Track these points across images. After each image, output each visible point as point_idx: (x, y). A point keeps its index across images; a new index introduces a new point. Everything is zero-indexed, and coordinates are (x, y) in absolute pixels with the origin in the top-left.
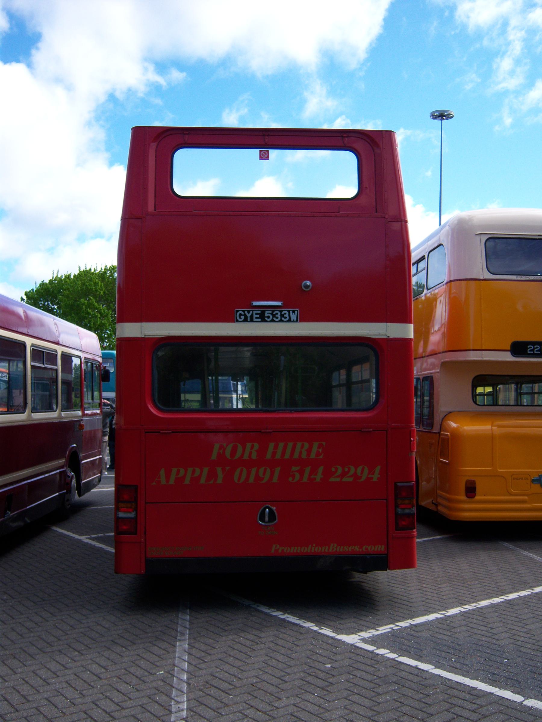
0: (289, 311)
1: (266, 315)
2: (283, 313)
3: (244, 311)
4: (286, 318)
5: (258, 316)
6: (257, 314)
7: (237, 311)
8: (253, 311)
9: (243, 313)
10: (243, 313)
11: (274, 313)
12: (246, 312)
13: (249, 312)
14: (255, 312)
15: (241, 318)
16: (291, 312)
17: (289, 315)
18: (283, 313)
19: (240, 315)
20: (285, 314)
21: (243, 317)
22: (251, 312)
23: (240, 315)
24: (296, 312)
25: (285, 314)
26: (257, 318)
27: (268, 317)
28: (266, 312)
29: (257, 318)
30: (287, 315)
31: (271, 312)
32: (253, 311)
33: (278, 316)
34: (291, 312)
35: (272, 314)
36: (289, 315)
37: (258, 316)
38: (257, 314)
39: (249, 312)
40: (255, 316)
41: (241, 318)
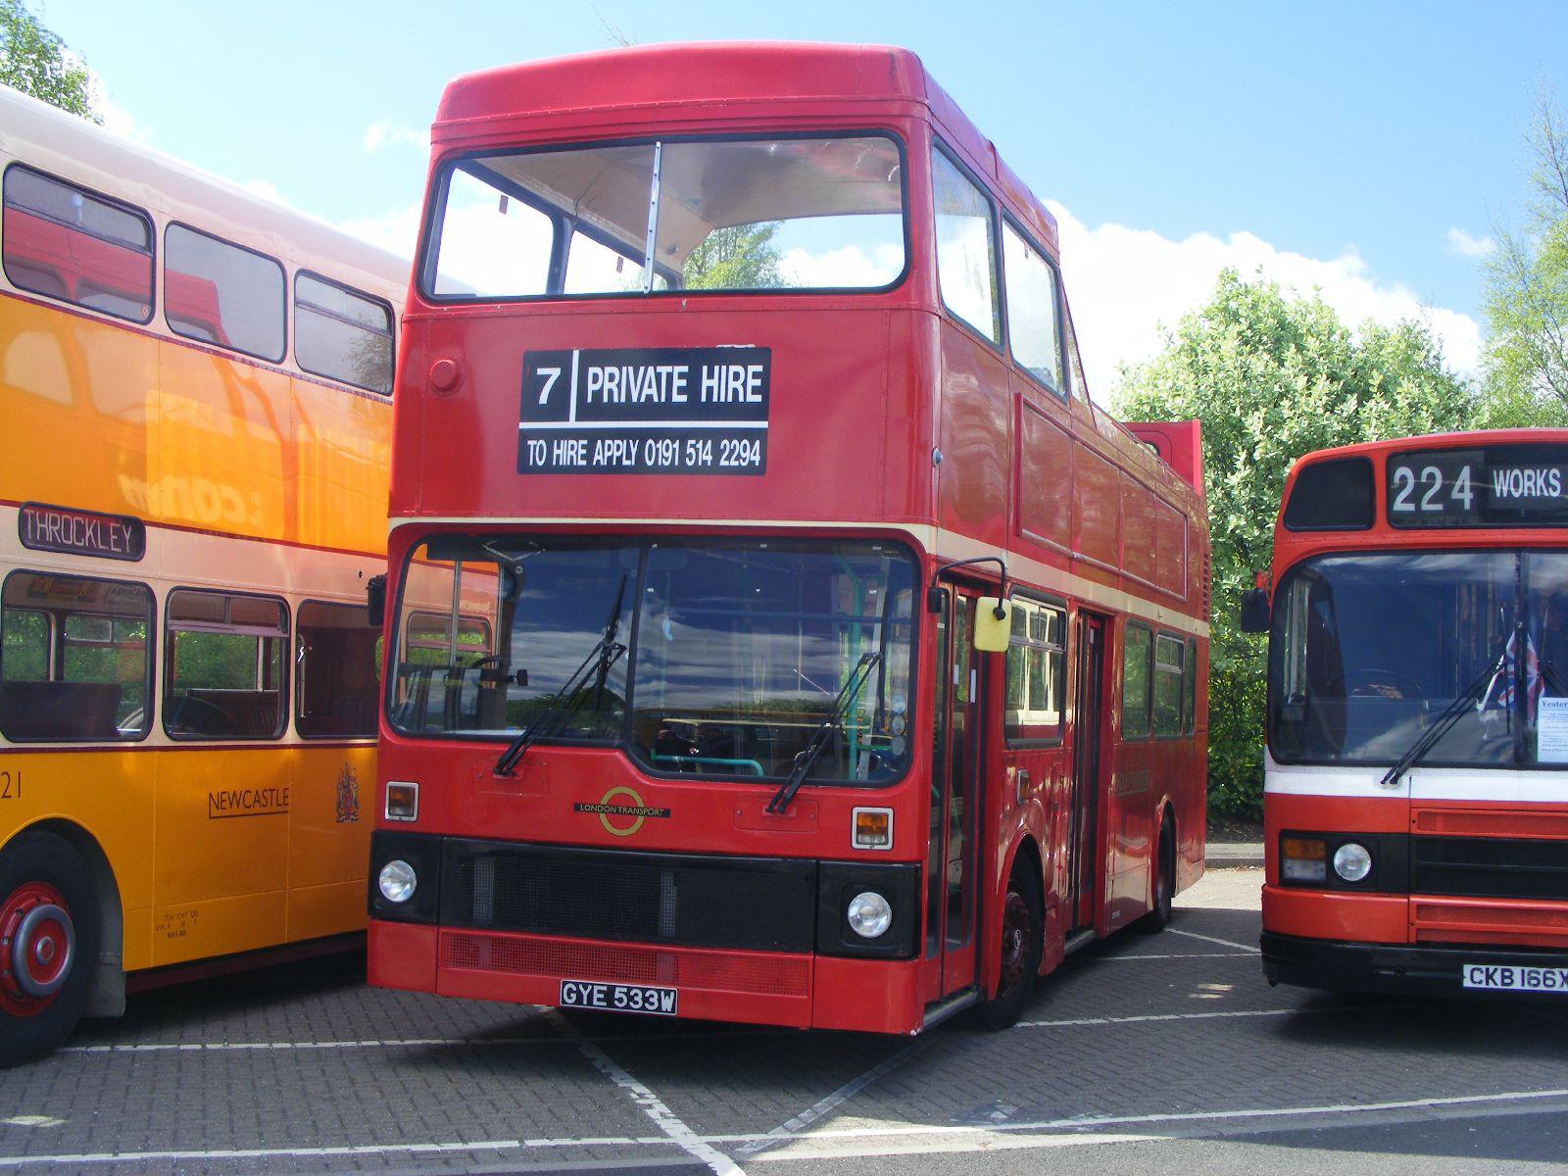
0: (659, 992)
1: (617, 995)
2: (647, 995)
3: (577, 984)
4: (652, 1004)
5: (602, 996)
6: (599, 992)
7: (565, 983)
9: (575, 989)
10: (575, 989)
11: (632, 994)
12: (581, 986)
14: (596, 988)
15: (570, 997)
16: (663, 993)
17: (659, 1000)
18: (647, 995)
19: (570, 990)
20: (652, 996)
21: (574, 996)
22: (590, 987)
23: (570, 990)
24: (672, 994)
25: (652, 996)
26: (599, 1000)
27: (621, 1000)
28: (618, 990)
30: (654, 1000)
31: (625, 990)
32: (593, 985)
33: (638, 999)
34: (663, 993)
35: (627, 994)
36: (659, 1000)
37: (602, 996)
38: (599, 992)
39: (585, 986)
40: (596, 995)
41: (570, 997)
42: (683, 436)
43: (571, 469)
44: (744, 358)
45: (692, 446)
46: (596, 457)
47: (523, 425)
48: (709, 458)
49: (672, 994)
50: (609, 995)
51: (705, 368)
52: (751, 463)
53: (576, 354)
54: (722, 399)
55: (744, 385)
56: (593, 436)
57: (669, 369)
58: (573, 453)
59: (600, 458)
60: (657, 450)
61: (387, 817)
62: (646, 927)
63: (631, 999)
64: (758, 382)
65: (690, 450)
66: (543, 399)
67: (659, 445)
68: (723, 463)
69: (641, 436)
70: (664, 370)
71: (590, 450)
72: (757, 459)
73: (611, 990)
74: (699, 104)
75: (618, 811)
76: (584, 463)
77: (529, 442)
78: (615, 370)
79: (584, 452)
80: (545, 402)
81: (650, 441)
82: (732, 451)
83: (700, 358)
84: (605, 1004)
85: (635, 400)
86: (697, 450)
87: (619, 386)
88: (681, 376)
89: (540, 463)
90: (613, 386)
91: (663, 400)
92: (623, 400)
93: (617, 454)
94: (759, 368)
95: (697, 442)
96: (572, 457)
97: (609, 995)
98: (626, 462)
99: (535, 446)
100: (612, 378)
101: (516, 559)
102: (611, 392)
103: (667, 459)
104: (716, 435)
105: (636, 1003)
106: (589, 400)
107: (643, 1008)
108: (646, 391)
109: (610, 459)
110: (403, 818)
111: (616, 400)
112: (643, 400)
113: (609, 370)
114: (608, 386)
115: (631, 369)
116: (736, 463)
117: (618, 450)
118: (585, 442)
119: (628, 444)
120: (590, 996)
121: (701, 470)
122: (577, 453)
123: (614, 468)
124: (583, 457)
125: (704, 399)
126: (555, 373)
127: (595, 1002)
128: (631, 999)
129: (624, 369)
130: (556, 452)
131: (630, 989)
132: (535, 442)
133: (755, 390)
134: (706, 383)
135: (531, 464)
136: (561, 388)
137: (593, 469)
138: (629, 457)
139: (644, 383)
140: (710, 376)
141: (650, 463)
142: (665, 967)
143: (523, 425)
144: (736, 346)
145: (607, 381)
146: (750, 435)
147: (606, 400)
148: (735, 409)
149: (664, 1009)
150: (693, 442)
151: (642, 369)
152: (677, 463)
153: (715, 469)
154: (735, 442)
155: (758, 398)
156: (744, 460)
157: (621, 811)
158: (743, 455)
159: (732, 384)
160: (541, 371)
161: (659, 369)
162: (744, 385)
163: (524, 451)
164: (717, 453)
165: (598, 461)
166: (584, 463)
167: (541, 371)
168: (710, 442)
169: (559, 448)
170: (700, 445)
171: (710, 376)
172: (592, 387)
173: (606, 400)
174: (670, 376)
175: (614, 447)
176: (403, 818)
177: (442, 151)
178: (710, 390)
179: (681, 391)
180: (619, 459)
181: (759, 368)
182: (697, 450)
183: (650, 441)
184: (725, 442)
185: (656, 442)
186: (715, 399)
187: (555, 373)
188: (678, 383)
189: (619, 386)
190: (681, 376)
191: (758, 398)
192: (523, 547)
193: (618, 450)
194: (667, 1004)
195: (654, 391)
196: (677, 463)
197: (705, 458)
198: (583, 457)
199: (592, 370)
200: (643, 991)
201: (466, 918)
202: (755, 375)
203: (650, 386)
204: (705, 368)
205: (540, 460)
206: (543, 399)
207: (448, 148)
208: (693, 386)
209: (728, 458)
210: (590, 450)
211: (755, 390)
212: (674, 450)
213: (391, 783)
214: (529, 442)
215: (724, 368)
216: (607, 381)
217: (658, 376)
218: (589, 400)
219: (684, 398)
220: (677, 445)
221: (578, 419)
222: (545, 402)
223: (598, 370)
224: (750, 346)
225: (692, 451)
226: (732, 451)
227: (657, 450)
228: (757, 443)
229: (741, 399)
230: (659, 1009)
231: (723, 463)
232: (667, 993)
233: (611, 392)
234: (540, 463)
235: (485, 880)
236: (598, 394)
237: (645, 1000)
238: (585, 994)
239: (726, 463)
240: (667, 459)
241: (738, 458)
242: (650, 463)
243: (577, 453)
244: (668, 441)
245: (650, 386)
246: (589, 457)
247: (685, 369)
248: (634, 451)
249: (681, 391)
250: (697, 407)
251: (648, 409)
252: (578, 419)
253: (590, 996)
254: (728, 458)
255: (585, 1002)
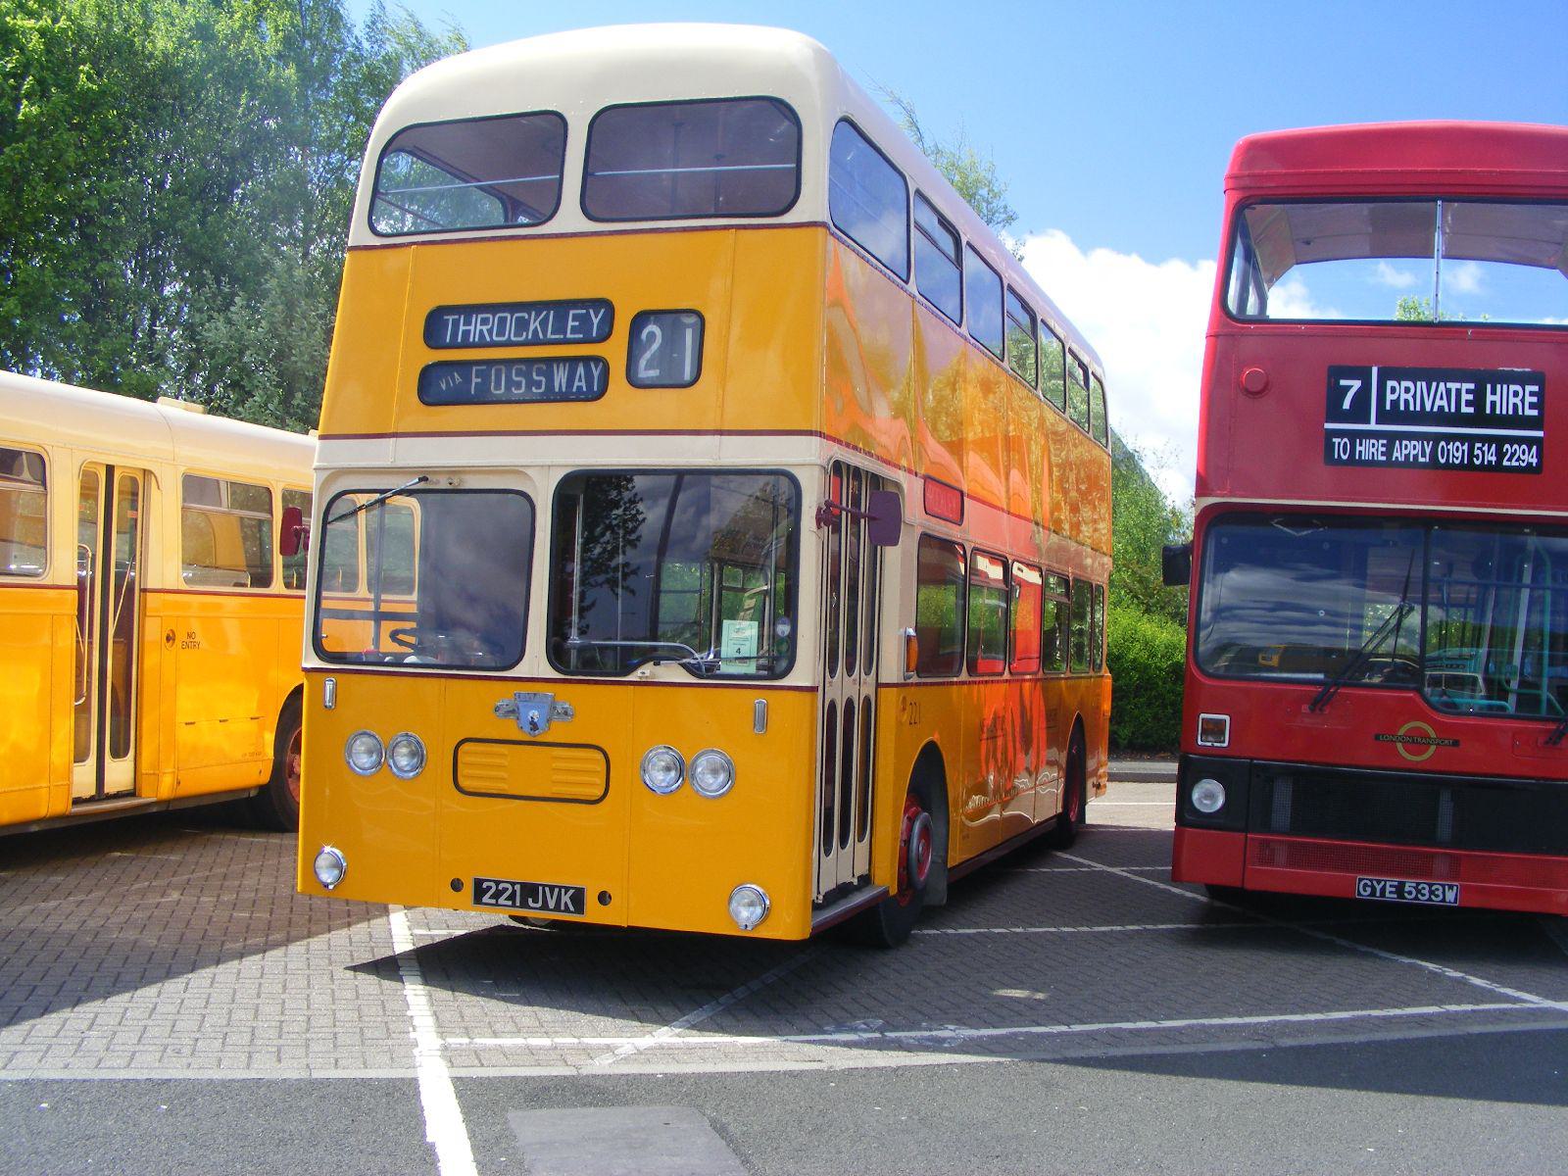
0: (1443, 886)
1: (1407, 889)
3: (1371, 880)
4: (1437, 896)
5: (1394, 889)
6: (1391, 886)
7: (1361, 880)
8: (1385, 881)
9: (1369, 883)
10: (1369, 883)
11: (1420, 887)
12: (1375, 882)
13: (1379, 882)
14: (1388, 884)
15: (1365, 890)
18: (1433, 888)
19: (1366, 885)
20: (1437, 889)
21: (1369, 890)
22: (1383, 883)
23: (1366, 885)
24: (1455, 888)
25: (1437, 889)
26: (1391, 892)
27: (1410, 893)
28: (1407, 885)
29: (1391, 892)
30: (1440, 893)
31: (1414, 885)
32: (1385, 881)
33: (1426, 892)
35: (1416, 888)
37: (1394, 889)
38: (1391, 886)
39: (1379, 882)
40: (1388, 889)
41: (1365, 890)
42: (1471, 440)
43: (1372, 463)
44: (1523, 380)
45: (1478, 448)
46: (1395, 454)
47: (1328, 426)
48: (1494, 459)
49: (1455, 888)
50: (1400, 889)
51: (1489, 386)
52: (1530, 464)
53: (1375, 370)
54: (1504, 412)
55: (1523, 401)
56: (1392, 438)
57: (1458, 385)
58: (1374, 450)
59: (1398, 455)
60: (1448, 450)
61: (1200, 743)
62: (1430, 839)
63: (1419, 891)
64: (1534, 399)
65: (1476, 452)
66: (1346, 405)
67: (1450, 447)
68: (1505, 463)
69: (1436, 438)
70: (1454, 386)
71: (1390, 448)
72: (1534, 461)
73: (1402, 885)
74: (1475, 172)
75: (1413, 740)
76: (1384, 458)
77: (1334, 440)
78: (1410, 384)
79: (1384, 449)
80: (1348, 408)
81: (1443, 443)
82: (1513, 455)
83: (1483, 380)
84: (1395, 896)
85: (1428, 409)
86: (1483, 452)
87: (1414, 397)
88: (1468, 391)
89: (1345, 457)
90: (1409, 397)
91: (1453, 410)
92: (1418, 408)
93: (1413, 452)
94: (1535, 388)
95: (1483, 446)
96: (1373, 453)
97: (1400, 889)
98: (1421, 460)
99: (1339, 444)
100: (1407, 390)
101: (1300, 534)
102: (1406, 402)
103: (1457, 458)
104: (1500, 441)
105: (1423, 895)
106: (1388, 407)
107: (1430, 899)
108: (1438, 403)
109: (1407, 456)
110: (1216, 744)
111: (1412, 408)
112: (1435, 409)
113: (1404, 384)
114: (1403, 396)
115: (1424, 384)
116: (1517, 464)
117: (1414, 449)
118: (1385, 442)
119: (1423, 443)
120: (1383, 890)
121: (1487, 468)
122: (1377, 450)
123: (1410, 464)
124: (1383, 454)
125: (1488, 411)
126: (1356, 384)
127: (1387, 895)
128: (1419, 891)
129: (1419, 383)
130: (1358, 448)
131: (1418, 884)
132: (1340, 440)
133: (1532, 406)
134: (1489, 398)
135: (1336, 456)
136: (1363, 396)
137: (1390, 463)
138: (1424, 455)
139: (1437, 397)
140: (1494, 392)
141: (1443, 461)
142: (1440, 866)
143: (1328, 426)
144: (1516, 370)
145: (1403, 392)
146: (1529, 442)
147: (1402, 408)
148: (1516, 420)
149: (1447, 900)
150: (1480, 445)
151: (1434, 384)
152: (1466, 462)
153: (1498, 467)
154: (1516, 446)
155: (1535, 413)
156: (1523, 461)
157: (1416, 742)
158: (1522, 457)
159: (1512, 400)
160: (1343, 382)
161: (1449, 385)
162: (1523, 401)
163: (1330, 447)
164: (1500, 455)
165: (1397, 458)
166: (1384, 458)
167: (1343, 382)
168: (1494, 445)
169: (1361, 445)
170: (1485, 448)
171: (1494, 392)
172: (1390, 397)
173: (1402, 408)
174: (1458, 391)
175: (1410, 447)
176: (1216, 744)
177: (1240, 196)
178: (1493, 404)
179: (1468, 403)
180: (1416, 457)
181: (1535, 388)
182: (1483, 452)
183: (1443, 443)
184: (1507, 446)
185: (1447, 444)
186: (1498, 412)
187: (1356, 384)
188: (1465, 397)
189: (1414, 397)
190: (1468, 391)
191: (1535, 413)
192: (1308, 525)
193: (1414, 449)
194: (1450, 896)
195: (1444, 403)
196: (1466, 462)
197: (1490, 459)
198: (1383, 454)
199: (1390, 384)
200: (1430, 885)
201: (1266, 826)
202: (1532, 394)
203: (1441, 398)
204: (1489, 386)
205: (1345, 454)
206: (1346, 405)
207: (1247, 195)
208: (1478, 400)
209: (1510, 460)
210: (1390, 448)
211: (1532, 406)
212: (1463, 451)
213: (1203, 716)
214: (1334, 440)
215: (1505, 386)
216: (1403, 392)
217: (1449, 391)
218: (1388, 407)
219: (1471, 410)
220: (1465, 447)
221: (1377, 423)
222: (1348, 408)
223: (1394, 383)
224: (1527, 370)
225: (1479, 452)
226: (1513, 455)
227: (1448, 450)
228: (1534, 448)
229: (1520, 413)
230: (1444, 900)
231: (1505, 463)
232: (1451, 887)
233: (1406, 402)
234: (1345, 457)
235: (1283, 796)
236: (1395, 403)
237: (1431, 892)
238: (1378, 888)
239: (1508, 464)
240: (1457, 458)
241: (1518, 459)
242: (1443, 461)
243: (1377, 450)
244: (1458, 444)
245: (1441, 398)
246: (1388, 453)
247: (1472, 386)
248: (1428, 451)
249: (1468, 403)
250: (1480, 418)
251: (1440, 417)
252: (1377, 423)
253: (1383, 890)
254: (1510, 460)
255: (1378, 894)
